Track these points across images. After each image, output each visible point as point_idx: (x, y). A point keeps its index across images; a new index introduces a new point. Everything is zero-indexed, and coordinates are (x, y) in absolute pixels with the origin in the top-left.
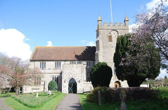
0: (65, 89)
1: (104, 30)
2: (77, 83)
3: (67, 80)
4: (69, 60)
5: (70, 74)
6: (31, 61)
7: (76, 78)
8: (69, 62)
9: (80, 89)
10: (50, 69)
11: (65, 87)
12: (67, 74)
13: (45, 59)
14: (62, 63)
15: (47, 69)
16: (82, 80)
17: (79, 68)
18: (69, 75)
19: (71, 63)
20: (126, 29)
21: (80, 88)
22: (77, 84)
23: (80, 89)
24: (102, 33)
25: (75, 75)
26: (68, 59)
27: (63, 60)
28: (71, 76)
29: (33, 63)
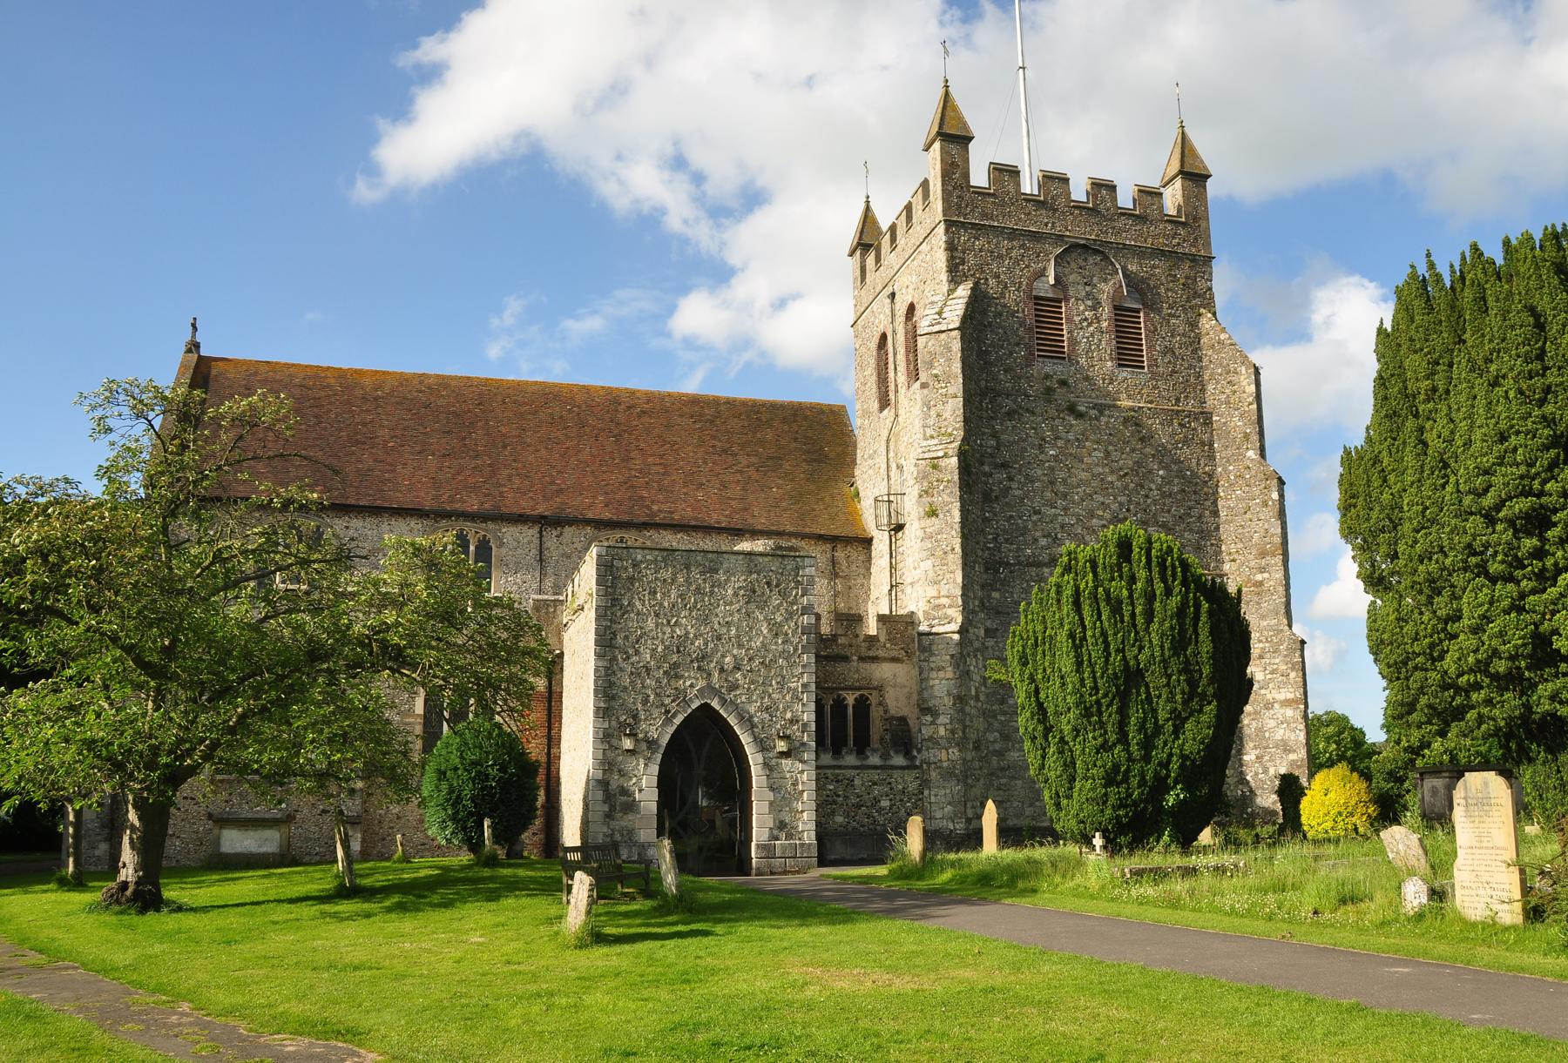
4: (590, 515)
18: (674, 673)
27: (520, 519)
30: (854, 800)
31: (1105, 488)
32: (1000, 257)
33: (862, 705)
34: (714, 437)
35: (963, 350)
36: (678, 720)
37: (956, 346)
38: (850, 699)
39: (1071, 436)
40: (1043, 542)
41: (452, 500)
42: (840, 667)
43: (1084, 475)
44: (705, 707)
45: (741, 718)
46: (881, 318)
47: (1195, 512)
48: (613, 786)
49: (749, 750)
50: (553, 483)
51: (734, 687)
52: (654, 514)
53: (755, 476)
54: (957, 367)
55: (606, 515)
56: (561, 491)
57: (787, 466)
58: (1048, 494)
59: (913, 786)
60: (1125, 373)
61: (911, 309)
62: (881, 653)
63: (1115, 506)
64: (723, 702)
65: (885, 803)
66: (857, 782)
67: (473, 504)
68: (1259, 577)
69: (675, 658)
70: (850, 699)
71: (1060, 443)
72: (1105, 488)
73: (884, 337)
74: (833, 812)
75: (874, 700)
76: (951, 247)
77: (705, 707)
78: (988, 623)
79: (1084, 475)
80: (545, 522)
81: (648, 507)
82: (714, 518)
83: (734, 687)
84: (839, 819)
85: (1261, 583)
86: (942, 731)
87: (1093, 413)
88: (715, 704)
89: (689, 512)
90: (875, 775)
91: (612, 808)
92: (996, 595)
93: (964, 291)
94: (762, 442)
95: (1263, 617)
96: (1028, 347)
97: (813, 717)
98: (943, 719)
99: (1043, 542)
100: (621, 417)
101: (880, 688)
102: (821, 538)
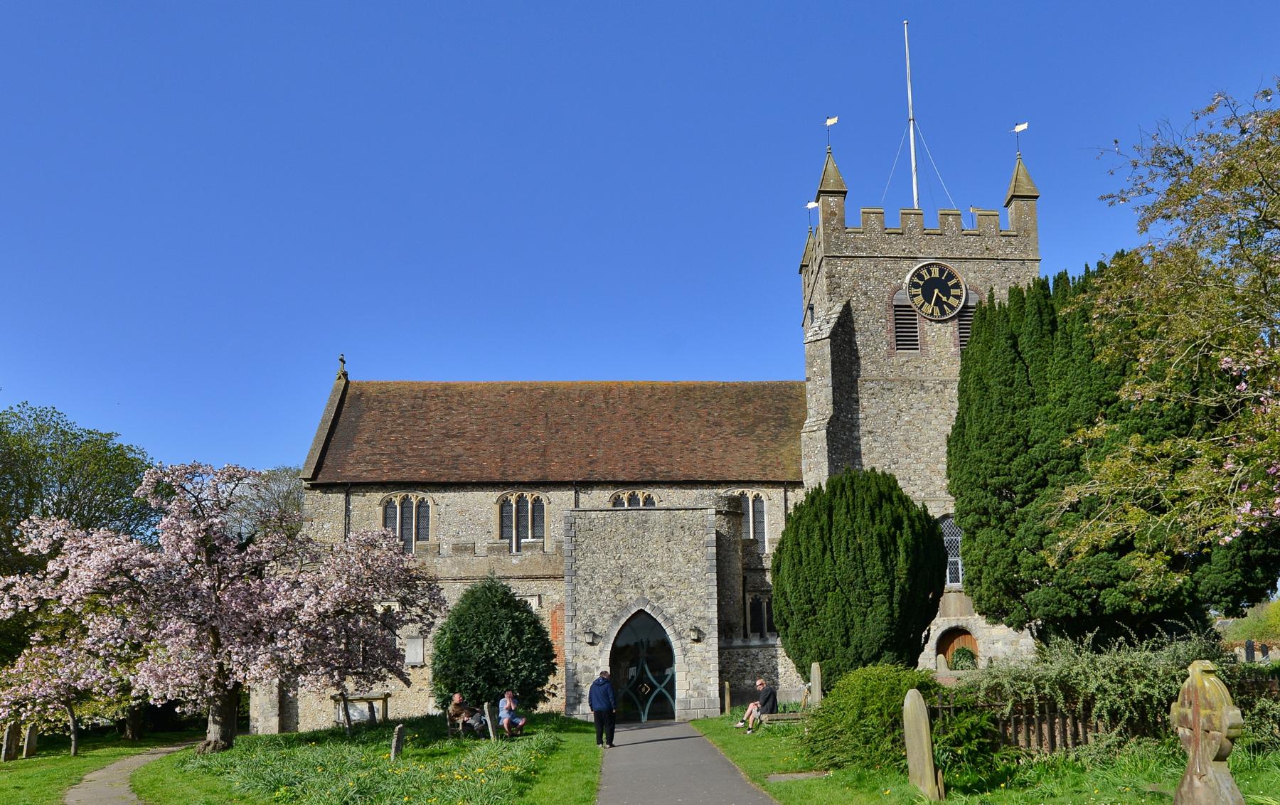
1: (861, 263)
2: (676, 645)
4: (610, 479)
6: (316, 484)
8: (600, 498)
9: (696, 688)
10: (459, 549)
12: (599, 582)
14: (558, 502)
15: (446, 549)
16: (709, 622)
19: (617, 502)
21: (697, 681)
26: (596, 477)
28: (632, 600)
29: (338, 499)
30: (758, 669)
32: (868, 279)
34: (709, 414)
35: (832, 353)
37: (827, 350)
39: (922, 406)
41: (514, 474)
50: (588, 456)
51: (660, 598)
52: (656, 474)
53: (733, 439)
54: (828, 366)
55: (621, 477)
56: (591, 463)
57: (759, 431)
58: (904, 449)
64: (653, 608)
66: (760, 656)
67: (530, 475)
69: (616, 581)
74: (744, 677)
76: (830, 276)
81: (653, 470)
82: (700, 474)
83: (660, 598)
87: (939, 387)
88: (648, 610)
93: (838, 308)
94: (743, 415)
97: (716, 615)
100: (644, 404)
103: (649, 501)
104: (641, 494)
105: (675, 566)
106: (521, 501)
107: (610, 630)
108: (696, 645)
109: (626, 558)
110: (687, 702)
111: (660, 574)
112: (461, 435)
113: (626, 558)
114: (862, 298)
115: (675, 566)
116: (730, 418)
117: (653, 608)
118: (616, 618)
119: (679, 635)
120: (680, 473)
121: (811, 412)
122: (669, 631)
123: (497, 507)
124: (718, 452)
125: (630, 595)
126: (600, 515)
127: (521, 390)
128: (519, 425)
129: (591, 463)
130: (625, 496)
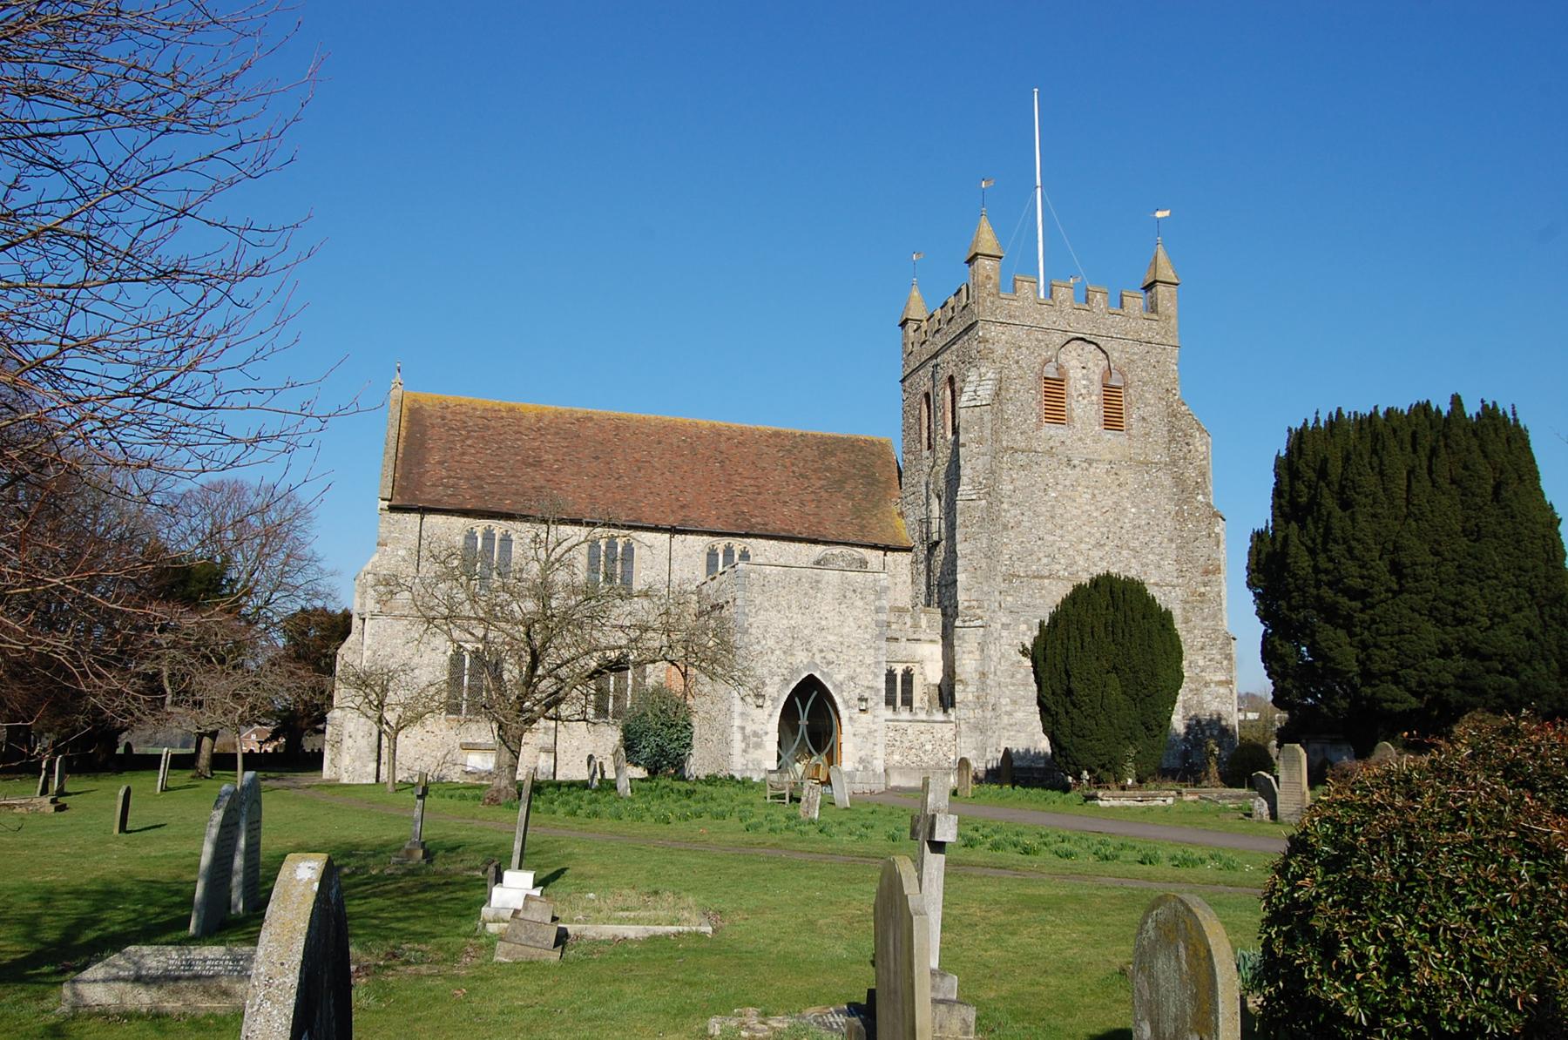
0: (755, 754)
1: (1014, 330)
2: (844, 713)
3: (770, 690)
5: (797, 643)
7: (839, 677)
9: (861, 760)
11: (758, 746)
12: (771, 643)
13: (507, 505)
17: (860, 603)
20: (1158, 339)
21: (862, 753)
22: (844, 721)
23: (861, 760)
24: (1000, 351)
25: (831, 656)
27: (656, 529)
31: (1091, 520)
33: (908, 677)
36: (793, 685)
38: (899, 670)
39: (1067, 483)
40: (1045, 560)
42: (893, 645)
43: (1075, 512)
44: (811, 677)
45: (835, 686)
46: (923, 382)
47: (1158, 540)
48: (748, 731)
49: (840, 707)
51: (829, 663)
52: (752, 526)
53: (825, 495)
56: (682, 507)
57: (848, 488)
58: (1049, 526)
59: (949, 735)
60: (1109, 435)
61: (951, 379)
62: (922, 637)
63: (1098, 535)
64: (823, 673)
65: (929, 747)
68: (1202, 590)
69: (788, 642)
70: (899, 670)
71: (1060, 488)
72: (1091, 520)
73: (927, 395)
75: (916, 671)
77: (811, 677)
78: (1004, 620)
79: (1075, 512)
80: (673, 531)
82: (797, 531)
83: (829, 663)
84: (897, 757)
85: (1202, 595)
86: (970, 697)
88: (818, 675)
89: (778, 525)
90: (922, 726)
91: (748, 745)
92: (1009, 599)
95: (1204, 619)
96: (1038, 416)
97: (883, 686)
98: (970, 689)
99: (1045, 560)
100: (723, 446)
101: (921, 662)
102: (875, 547)
103: (745, 556)
104: (738, 544)
105: (846, 630)
106: (611, 544)
107: (779, 692)
108: (862, 715)
109: (797, 619)
110: (851, 775)
111: (831, 638)
112: (538, 463)
113: (797, 619)
114: (1014, 366)
115: (846, 630)
116: (815, 471)
117: (823, 673)
118: (786, 682)
119: (845, 702)
120: (775, 526)
121: (964, 480)
122: (838, 700)
123: (704, 557)
124: (810, 508)
125: (801, 658)
126: (775, 570)
127: (591, 419)
128: (597, 458)
129: (682, 507)
130: (721, 543)
